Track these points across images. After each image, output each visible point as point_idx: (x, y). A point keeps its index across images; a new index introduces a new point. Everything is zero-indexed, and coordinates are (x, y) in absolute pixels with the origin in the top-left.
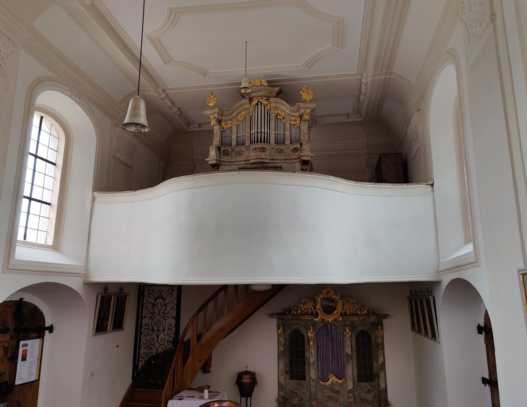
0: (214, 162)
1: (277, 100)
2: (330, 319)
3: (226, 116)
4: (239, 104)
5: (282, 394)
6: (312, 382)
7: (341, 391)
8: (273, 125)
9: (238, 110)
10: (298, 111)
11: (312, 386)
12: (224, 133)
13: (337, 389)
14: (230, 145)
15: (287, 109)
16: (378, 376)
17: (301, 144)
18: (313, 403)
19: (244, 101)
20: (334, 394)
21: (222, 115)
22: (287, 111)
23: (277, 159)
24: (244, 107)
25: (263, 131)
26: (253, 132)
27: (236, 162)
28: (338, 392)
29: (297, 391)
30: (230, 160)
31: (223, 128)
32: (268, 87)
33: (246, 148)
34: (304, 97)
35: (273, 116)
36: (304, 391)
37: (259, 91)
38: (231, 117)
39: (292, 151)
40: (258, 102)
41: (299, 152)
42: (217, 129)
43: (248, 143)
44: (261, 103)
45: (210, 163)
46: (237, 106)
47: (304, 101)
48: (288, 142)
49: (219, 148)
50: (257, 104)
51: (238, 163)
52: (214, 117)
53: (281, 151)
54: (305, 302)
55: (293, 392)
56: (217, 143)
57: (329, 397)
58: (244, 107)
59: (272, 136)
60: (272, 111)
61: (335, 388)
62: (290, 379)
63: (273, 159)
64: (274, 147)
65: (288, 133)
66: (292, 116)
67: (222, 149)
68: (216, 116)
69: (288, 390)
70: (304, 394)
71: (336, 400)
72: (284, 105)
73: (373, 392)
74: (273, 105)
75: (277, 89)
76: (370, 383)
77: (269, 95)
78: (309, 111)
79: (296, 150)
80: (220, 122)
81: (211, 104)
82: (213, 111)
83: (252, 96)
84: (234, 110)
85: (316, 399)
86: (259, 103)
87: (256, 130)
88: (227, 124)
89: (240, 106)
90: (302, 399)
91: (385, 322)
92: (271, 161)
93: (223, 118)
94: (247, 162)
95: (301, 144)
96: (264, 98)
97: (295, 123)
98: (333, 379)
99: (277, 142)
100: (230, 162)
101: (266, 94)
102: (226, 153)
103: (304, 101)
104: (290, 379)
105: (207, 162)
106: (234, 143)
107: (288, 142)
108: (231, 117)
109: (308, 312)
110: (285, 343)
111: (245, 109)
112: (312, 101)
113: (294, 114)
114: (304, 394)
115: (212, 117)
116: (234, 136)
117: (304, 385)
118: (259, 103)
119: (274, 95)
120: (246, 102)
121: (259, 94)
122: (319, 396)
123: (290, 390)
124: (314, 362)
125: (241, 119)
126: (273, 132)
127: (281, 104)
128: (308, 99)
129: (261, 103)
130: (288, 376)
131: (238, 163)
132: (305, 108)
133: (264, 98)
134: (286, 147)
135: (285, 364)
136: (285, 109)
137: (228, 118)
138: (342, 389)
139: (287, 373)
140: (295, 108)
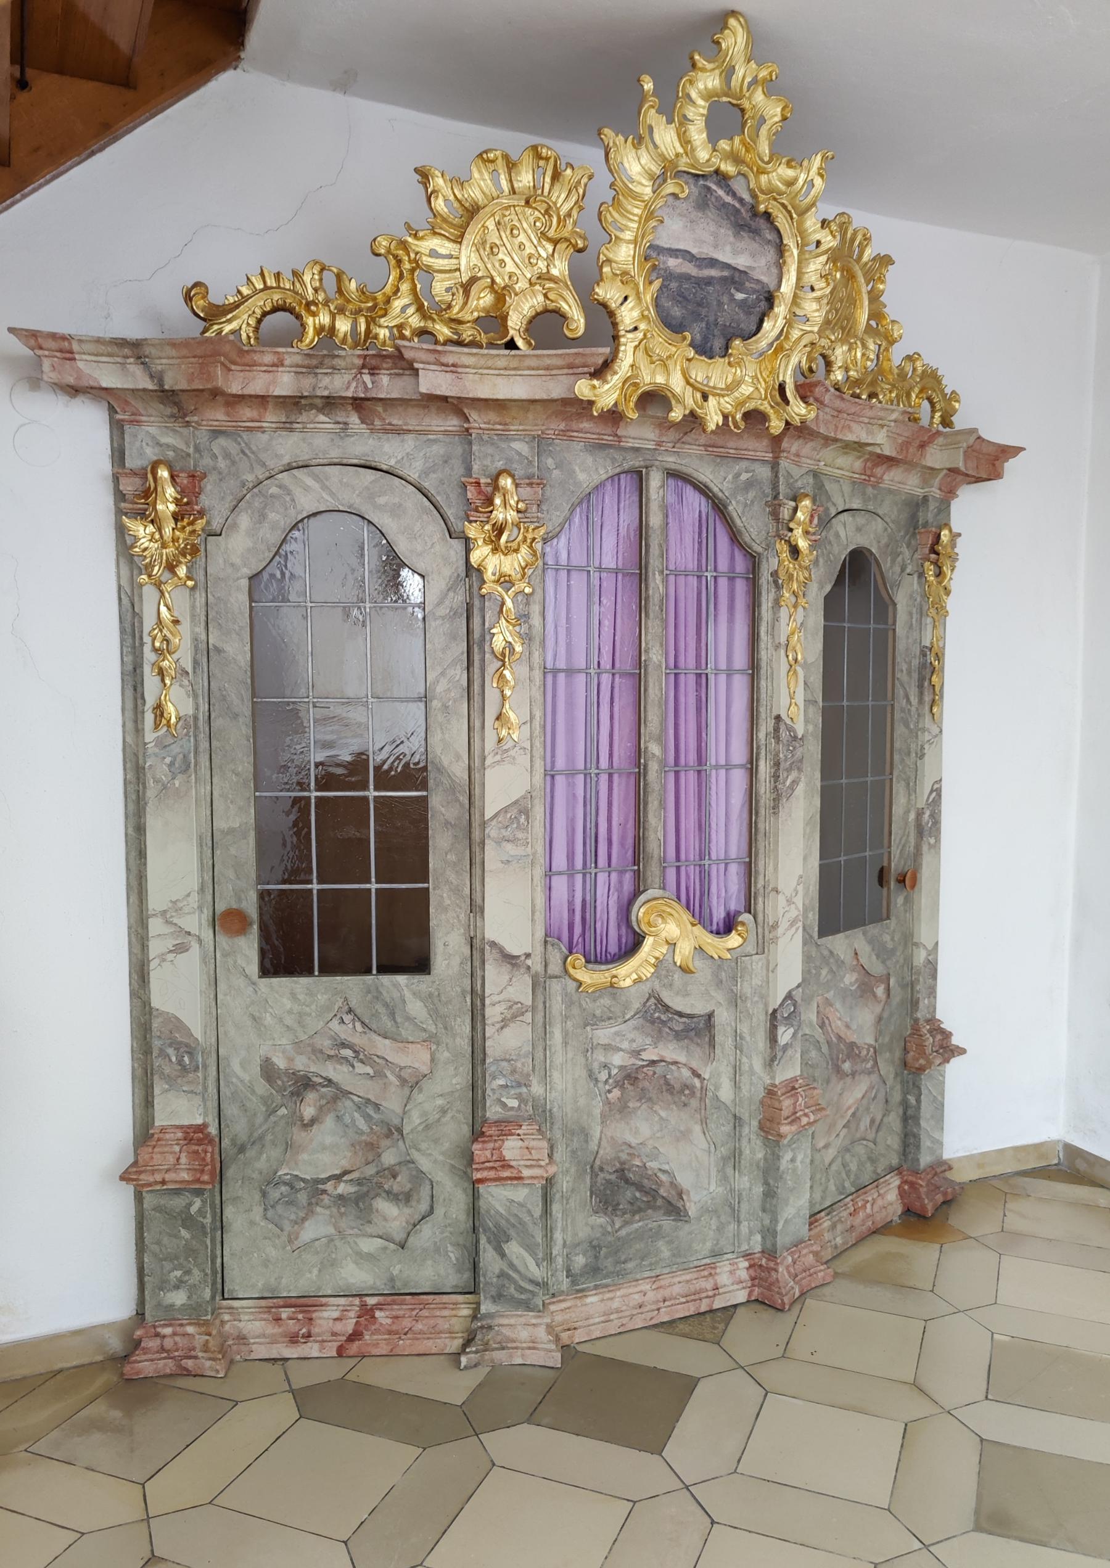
2: (729, 385)
5: (179, 1109)
6: (494, 976)
7: (723, 1017)
11: (493, 1013)
13: (696, 1006)
16: (907, 880)
18: (511, 1148)
20: (671, 1051)
28: (700, 1029)
29: (331, 1071)
36: (417, 1058)
54: (472, 211)
55: (303, 1084)
57: (630, 1077)
61: (677, 1003)
62: (265, 972)
69: (243, 1071)
70: (413, 1083)
71: (681, 1093)
73: (880, 991)
76: (873, 929)
85: (541, 1116)
90: (394, 1132)
91: (971, 512)
98: (671, 932)
104: (265, 972)
109: (495, 320)
110: (206, 653)
114: (413, 1083)
117: (416, 1008)
122: (566, 1086)
123: (268, 1071)
124: (521, 809)
130: (247, 949)
135: (211, 844)
138: (735, 1001)
139: (229, 922)
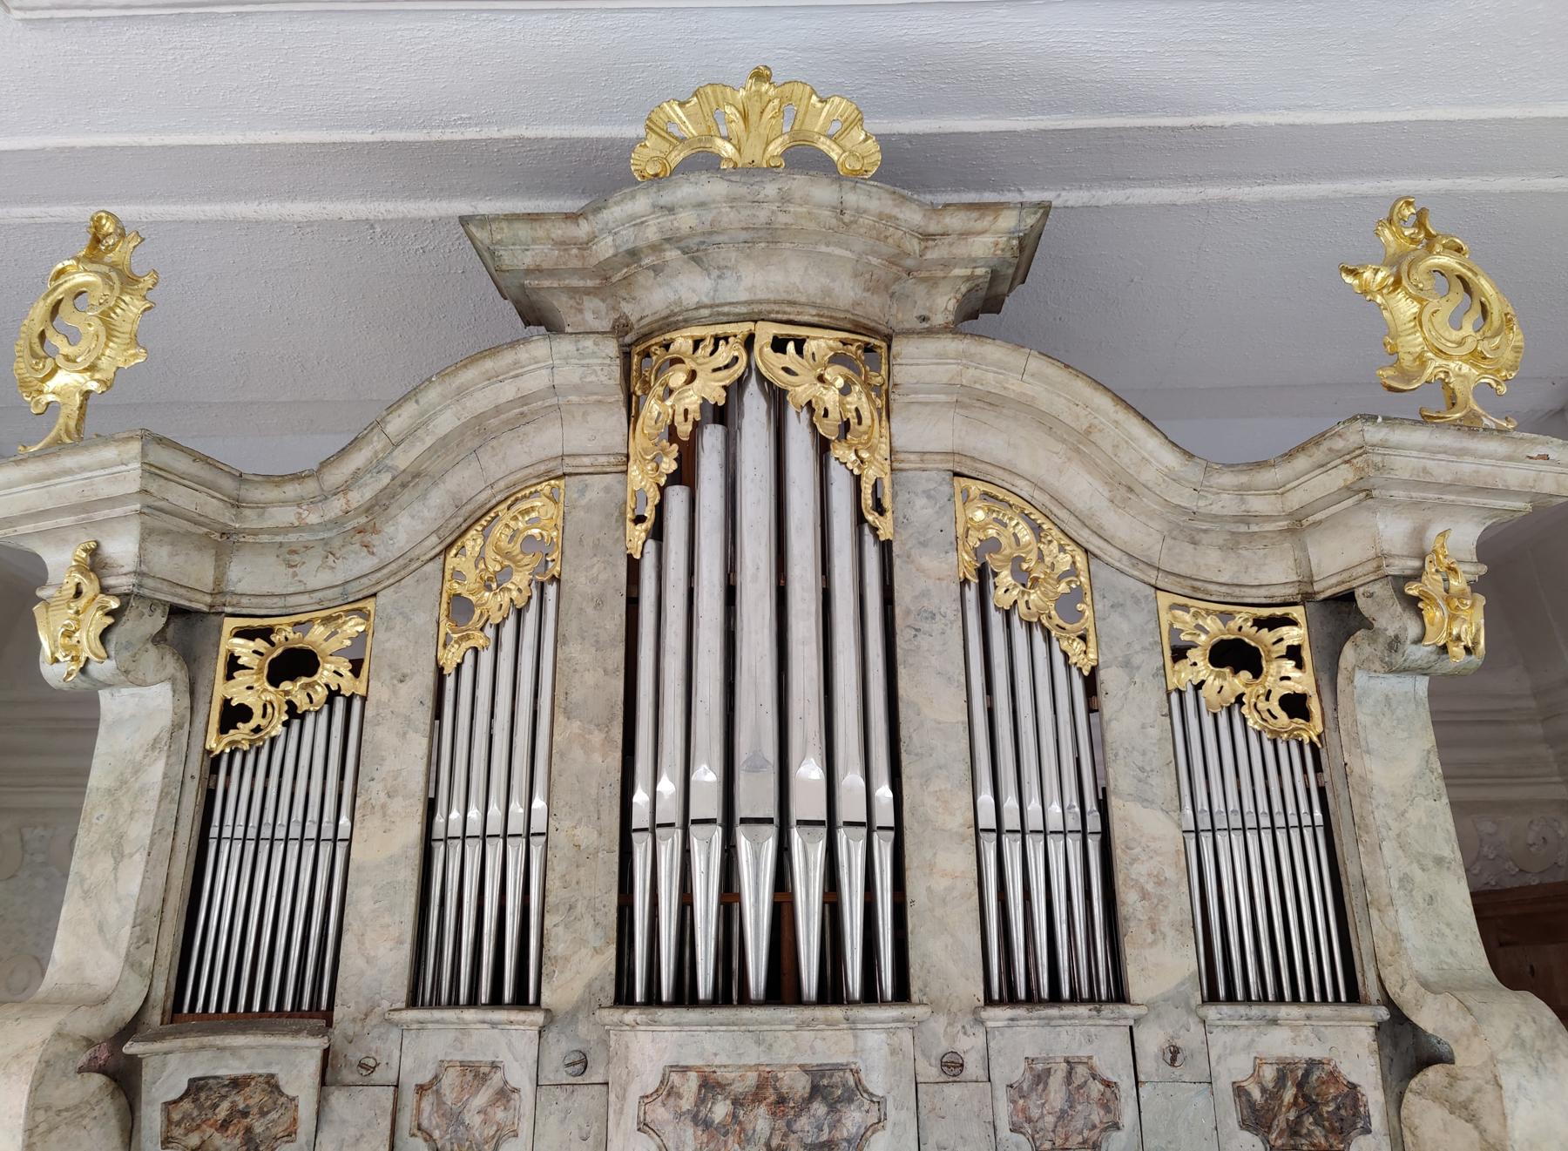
1: (993, 362)
3: (291, 555)
4: (481, 401)
9: (466, 482)
10: (1297, 526)
12: (238, 789)
14: (313, 1009)
15: (1125, 488)
19: (542, 363)
21: (224, 542)
24: (545, 441)
25: (808, 802)
26: (659, 793)
31: (233, 715)
32: (872, 202)
33: (559, 1047)
34: (1413, 343)
35: (930, 579)
37: (766, 239)
38: (356, 564)
40: (736, 389)
42: (139, 717)
43: (578, 963)
44: (777, 399)
46: (446, 422)
47: (1438, 408)
48: (1162, 963)
50: (723, 415)
52: (95, 563)
58: (545, 441)
60: (922, 511)
64: (969, 1045)
65: (1150, 834)
66: (1195, 591)
67: (170, 1069)
68: (122, 548)
72: (1080, 443)
74: (923, 431)
75: (986, 242)
77: (874, 309)
78: (1461, 537)
81: (67, 381)
82: (67, 490)
83: (652, 300)
84: (411, 480)
86: (754, 406)
87: (707, 775)
88: (295, 664)
89: (480, 432)
96: (821, 343)
97: (1240, 681)
101: (846, 293)
103: (1438, 408)
106: (375, 954)
107: (1162, 963)
108: (356, 564)
111: (558, 472)
113: (1214, 565)
115: (61, 561)
116: (384, 846)
118: (754, 406)
119: (944, 304)
120: (569, 374)
121: (751, 281)
125: (493, 603)
126: (943, 805)
127: (1046, 422)
128: (1462, 372)
129: (777, 399)
132: (1433, 496)
133: (821, 343)
134: (1151, 1041)
136: (1082, 488)
137: (318, 576)
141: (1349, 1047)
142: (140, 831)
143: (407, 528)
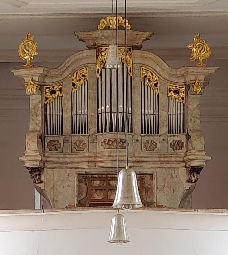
0: (36, 165)
3: (52, 77)
8: (137, 98)
9: (74, 67)
17: (188, 137)
22: (162, 73)
23: (147, 162)
24: (85, 61)
27: (72, 162)
30: (61, 160)
35: (137, 81)
39: (172, 146)
41: (184, 149)
45: (27, 164)
47: (196, 63)
49: (42, 138)
51: (76, 165)
53: (151, 146)
56: (38, 128)
59: (137, 119)
63: (138, 162)
66: (172, 83)
67: (48, 140)
72: (157, 63)
78: (202, 78)
79: (178, 145)
80: (41, 87)
88: (53, 92)
92: (136, 165)
93: (47, 80)
94: (92, 165)
95: (188, 137)
99: (144, 131)
100: (61, 163)
102: (55, 147)
105: (23, 162)
107: (163, 130)
112: (208, 62)
115: (28, 80)
126: (137, 111)
131: (76, 165)
132: (197, 74)
136: (158, 69)
140: (180, 72)
141: (183, 139)
142: (39, 113)
143: (66, 74)
